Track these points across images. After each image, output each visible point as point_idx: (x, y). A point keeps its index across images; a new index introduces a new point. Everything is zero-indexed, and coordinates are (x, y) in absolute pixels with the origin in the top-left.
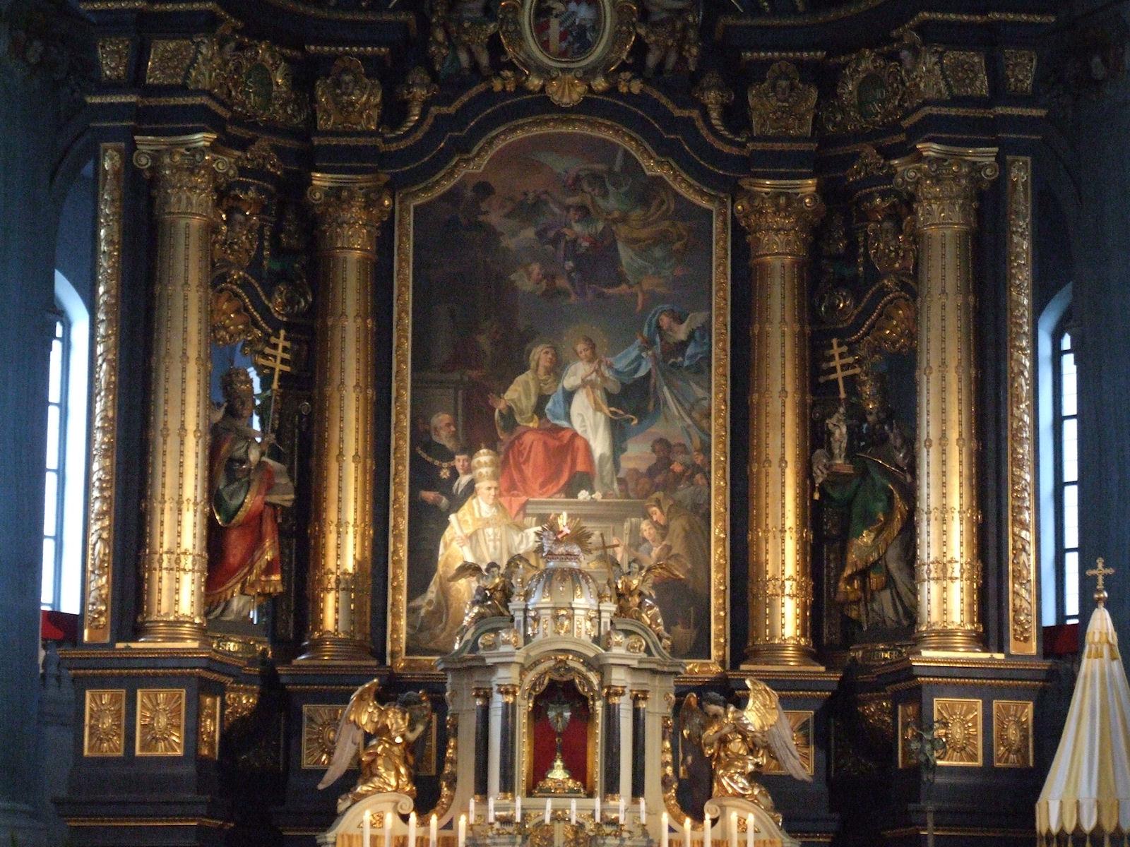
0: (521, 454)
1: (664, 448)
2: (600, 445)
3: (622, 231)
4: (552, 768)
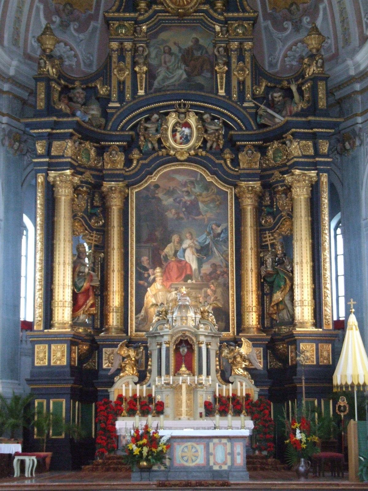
1: (214, 266)
2: (194, 266)
3: (200, 198)
4: (181, 367)
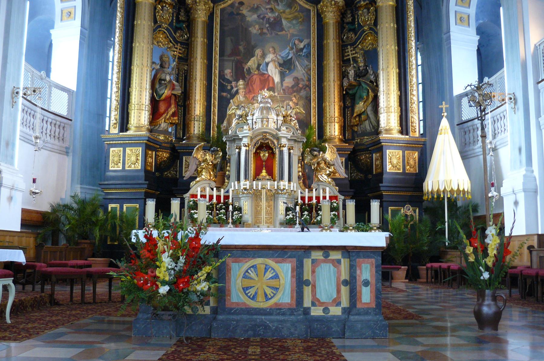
1: (297, 80)
2: (277, 79)
3: (283, 15)
4: (262, 172)
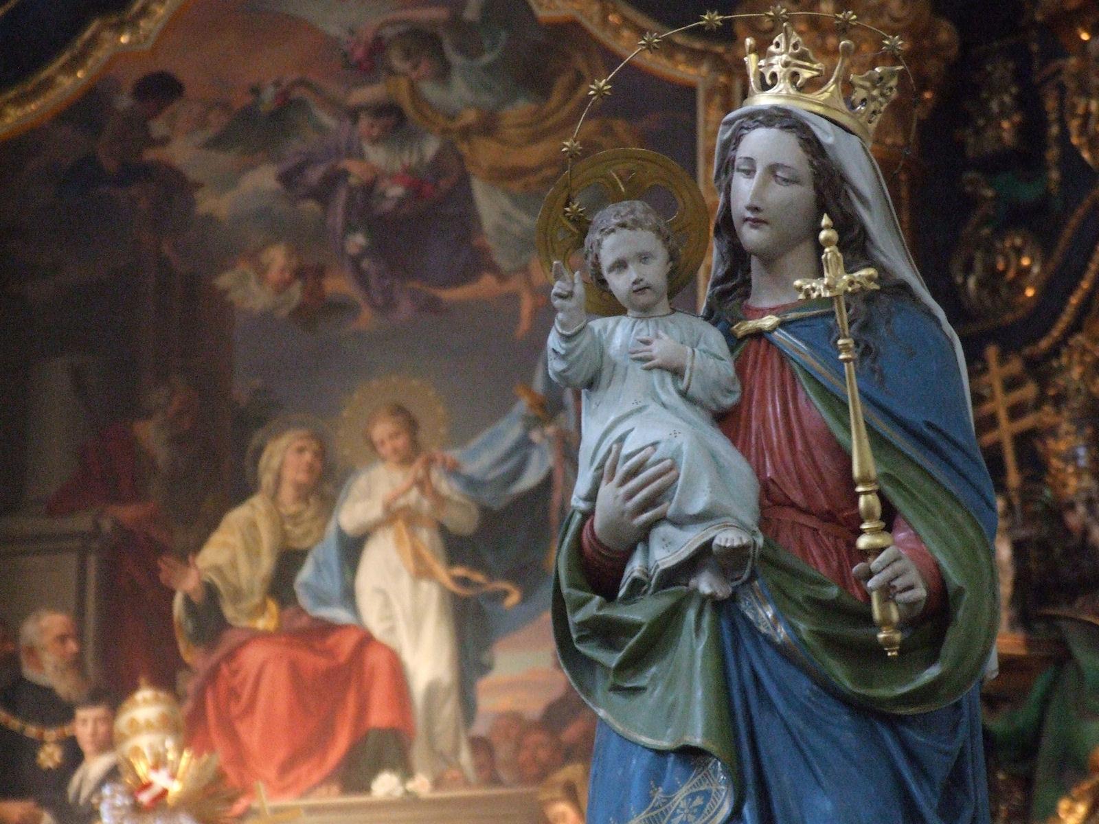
0: (234, 694)
3: (485, 152)
